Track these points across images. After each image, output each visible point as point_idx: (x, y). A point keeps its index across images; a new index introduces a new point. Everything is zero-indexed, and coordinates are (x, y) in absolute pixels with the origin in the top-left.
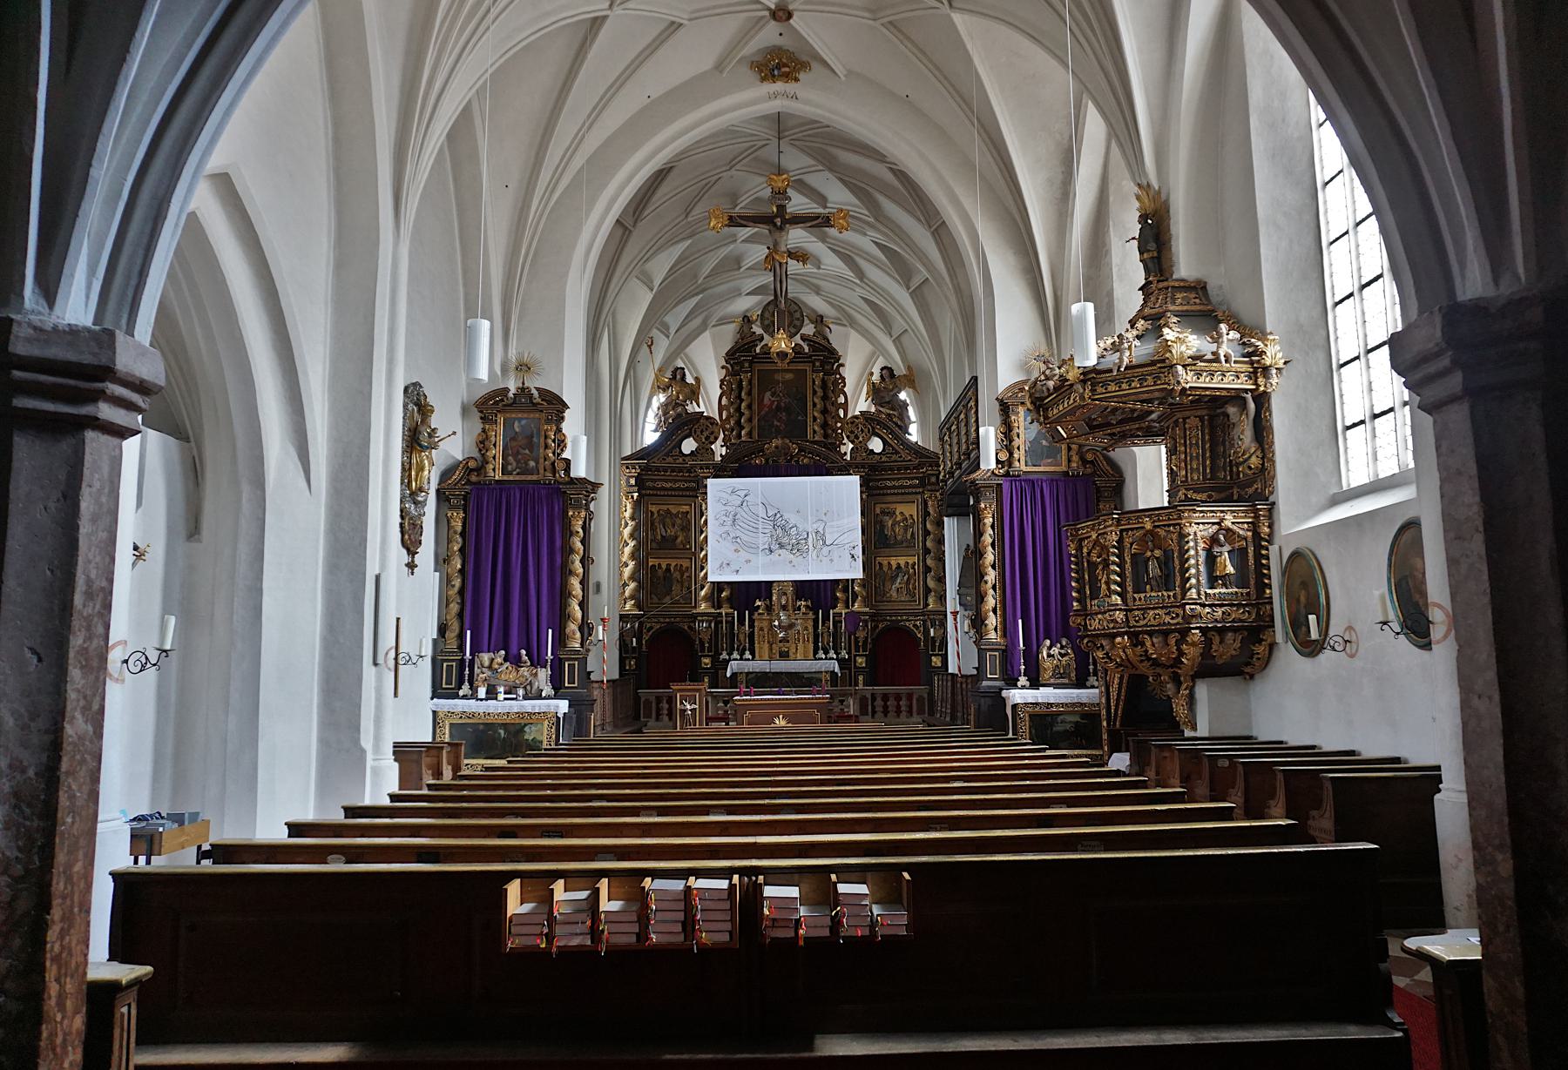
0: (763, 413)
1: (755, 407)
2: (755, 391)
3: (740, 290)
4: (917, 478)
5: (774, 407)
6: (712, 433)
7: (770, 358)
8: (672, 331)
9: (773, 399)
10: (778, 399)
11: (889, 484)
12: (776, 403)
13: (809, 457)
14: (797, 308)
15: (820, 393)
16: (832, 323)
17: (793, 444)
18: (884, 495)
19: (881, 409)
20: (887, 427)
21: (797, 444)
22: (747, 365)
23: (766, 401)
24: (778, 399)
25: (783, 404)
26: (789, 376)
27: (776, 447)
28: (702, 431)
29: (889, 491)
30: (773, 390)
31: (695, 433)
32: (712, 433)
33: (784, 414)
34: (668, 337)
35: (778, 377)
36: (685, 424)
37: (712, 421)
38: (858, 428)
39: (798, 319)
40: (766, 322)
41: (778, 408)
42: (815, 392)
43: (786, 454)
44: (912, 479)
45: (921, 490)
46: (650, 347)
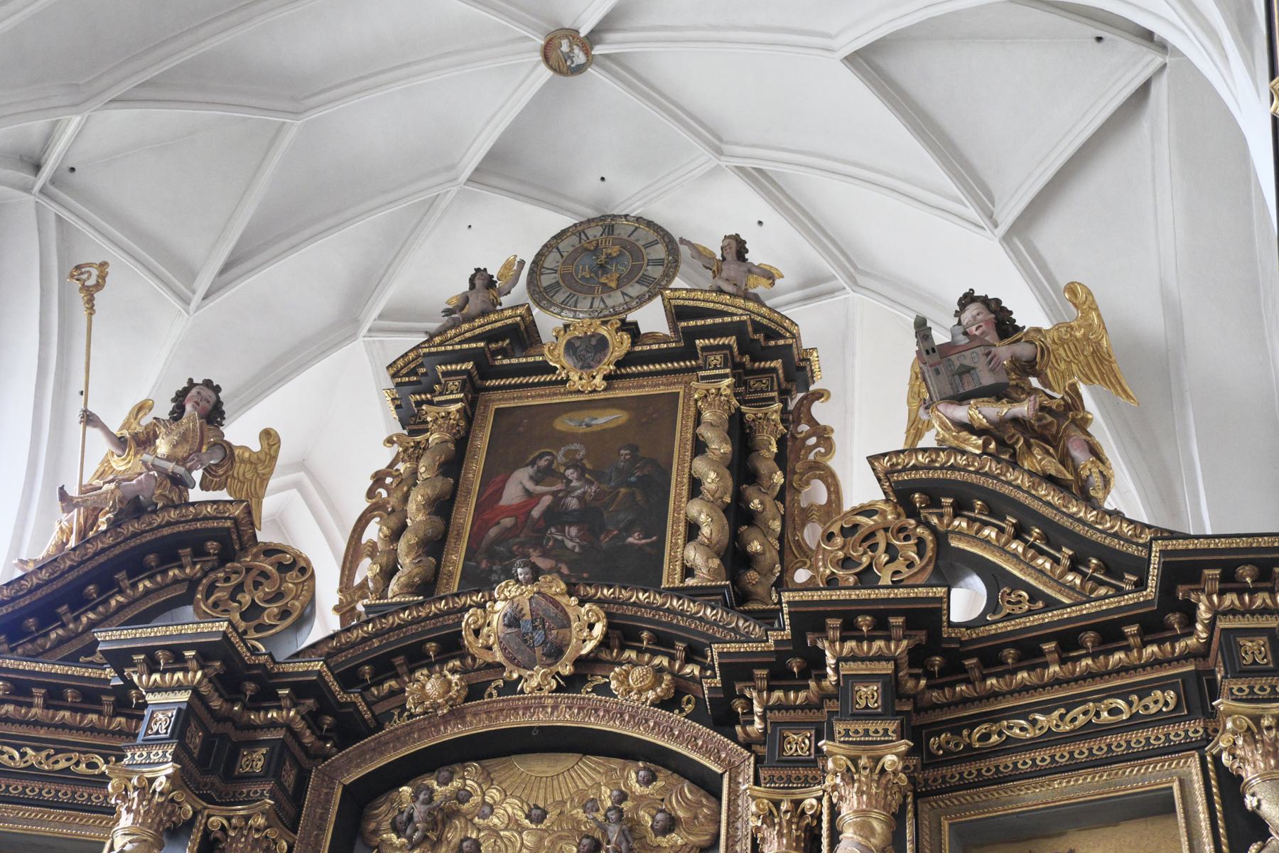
0: (493, 532)
1: (465, 515)
2: (475, 469)
3: (452, 167)
4: (1163, 685)
5: (536, 513)
6: (279, 596)
7: (545, 368)
8: (203, 285)
9: (540, 489)
10: (559, 487)
11: (1018, 729)
12: (547, 500)
13: (659, 670)
14: (652, 236)
15: (720, 447)
16: (788, 304)
17: (582, 603)
18: (1000, 779)
19: (961, 413)
20: (997, 506)
21: (600, 602)
22: (454, 384)
23: (512, 493)
24: (559, 487)
25: (573, 503)
26: (605, 419)
27: (513, 621)
28: (239, 588)
29: (1024, 761)
30: (543, 463)
31: (209, 593)
32: (279, 596)
33: (573, 531)
34: (186, 301)
35: (564, 424)
36: (168, 551)
37: (288, 559)
38: (873, 547)
39: (659, 262)
40: (546, 280)
41: (556, 515)
42: (699, 447)
43: (556, 652)
44: (1143, 691)
45: (1195, 728)
46: (90, 294)
